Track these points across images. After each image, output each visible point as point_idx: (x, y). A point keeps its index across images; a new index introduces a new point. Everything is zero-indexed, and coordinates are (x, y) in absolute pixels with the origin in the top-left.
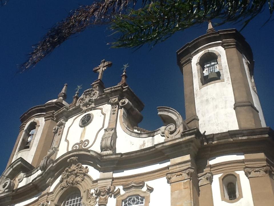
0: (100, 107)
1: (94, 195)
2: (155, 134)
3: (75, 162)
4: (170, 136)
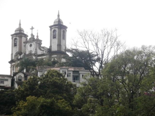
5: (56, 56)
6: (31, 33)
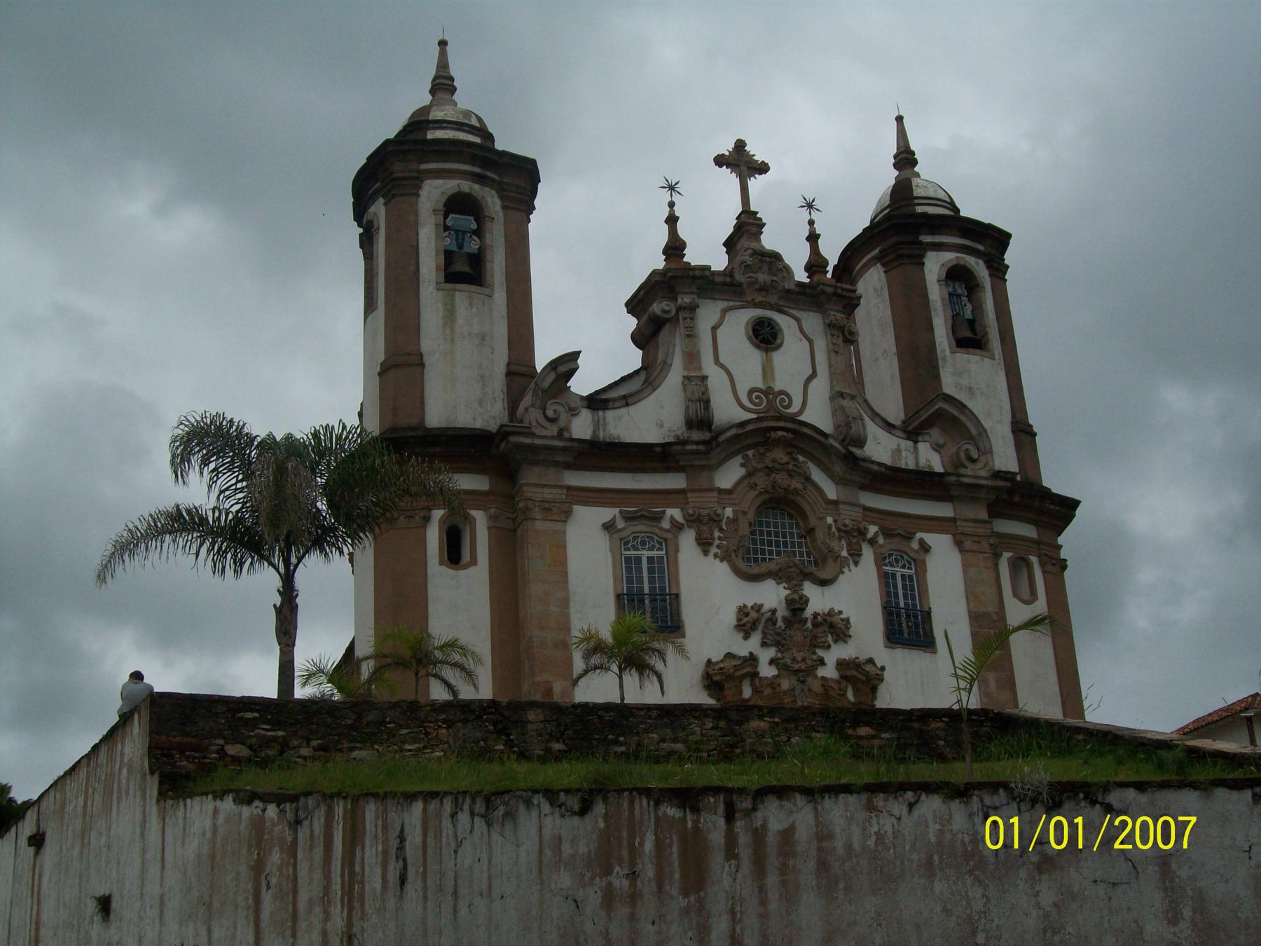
1: (834, 529)
2: (920, 438)
3: (787, 444)
4: (967, 463)
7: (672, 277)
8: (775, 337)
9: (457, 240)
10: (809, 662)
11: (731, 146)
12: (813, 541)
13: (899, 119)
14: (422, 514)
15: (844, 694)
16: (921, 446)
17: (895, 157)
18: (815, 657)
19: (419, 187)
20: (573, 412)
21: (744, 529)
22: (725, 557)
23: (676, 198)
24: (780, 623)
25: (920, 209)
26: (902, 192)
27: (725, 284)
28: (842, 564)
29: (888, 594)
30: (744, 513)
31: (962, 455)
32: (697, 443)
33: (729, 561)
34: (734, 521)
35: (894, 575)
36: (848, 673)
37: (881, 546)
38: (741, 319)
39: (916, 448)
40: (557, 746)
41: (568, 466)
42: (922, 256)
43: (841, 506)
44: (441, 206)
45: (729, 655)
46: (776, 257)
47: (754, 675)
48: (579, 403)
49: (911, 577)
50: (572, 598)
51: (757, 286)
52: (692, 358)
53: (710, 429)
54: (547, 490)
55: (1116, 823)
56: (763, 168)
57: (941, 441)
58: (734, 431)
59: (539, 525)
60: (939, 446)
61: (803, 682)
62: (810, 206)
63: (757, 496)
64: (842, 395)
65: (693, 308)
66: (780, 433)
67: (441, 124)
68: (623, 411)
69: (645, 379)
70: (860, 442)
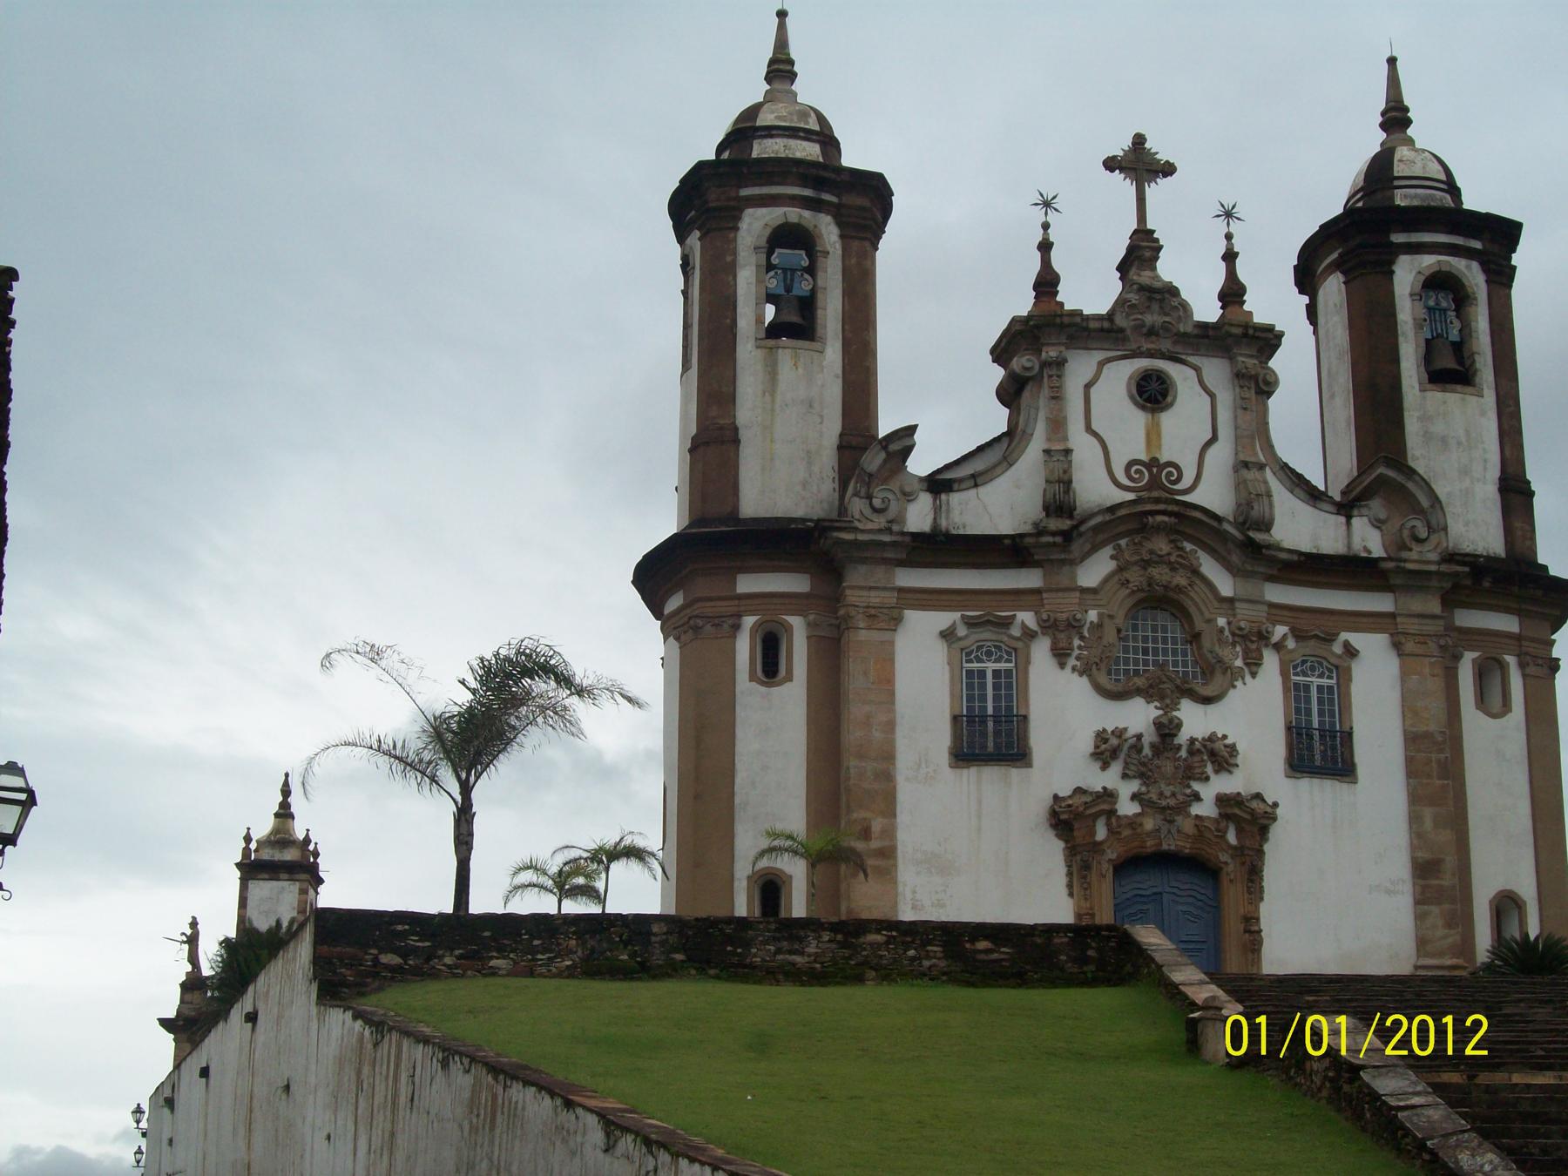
0: (1191, 359)
1: (1227, 633)
2: (1355, 512)
4: (1416, 548)
5: (1508, 623)
6: (1133, 225)
7: (1037, 327)
8: (1165, 394)
9: (785, 279)
10: (1181, 798)
11: (1127, 143)
12: (1200, 648)
13: (1392, 61)
14: (730, 622)
15: (1223, 837)
16: (1355, 521)
17: (1383, 114)
18: (1188, 791)
19: (738, 218)
20: (908, 497)
21: (1110, 636)
22: (1084, 671)
23: (1052, 217)
24: (1147, 751)
25: (1401, 199)
26: (1380, 172)
27: (1102, 330)
28: (1233, 677)
29: (1298, 711)
30: (1111, 617)
31: (1406, 533)
32: (1054, 534)
33: (1089, 676)
34: (1097, 627)
35: (1307, 687)
36: (1229, 811)
37: (1292, 651)
38: (1121, 373)
39: (1348, 523)
40: (679, 957)
41: (902, 563)
42: (1392, 262)
43: (1238, 605)
44: (763, 242)
45: (1079, 791)
46: (1172, 291)
47: (1112, 813)
48: (917, 486)
49: (1330, 688)
50: (898, 720)
51: (1145, 330)
52: (1058, 425)
53: (1071, 517)
54: (873, 593)
55: (1388, 1023)
56: (1168, 170)
57: (1382, 516)
58: (1099, 519)
59: (863, 635)
60: (1379, 521)
61: (1171, 822)
62: (1228, 214)
63: (1129, 595)
64: (1246, 465)
65: (1060, 363)
66: (1160, 518)
67: (770, 132)
68: (973, 492)
69: (1006, 446)
70: (1266, 525)
